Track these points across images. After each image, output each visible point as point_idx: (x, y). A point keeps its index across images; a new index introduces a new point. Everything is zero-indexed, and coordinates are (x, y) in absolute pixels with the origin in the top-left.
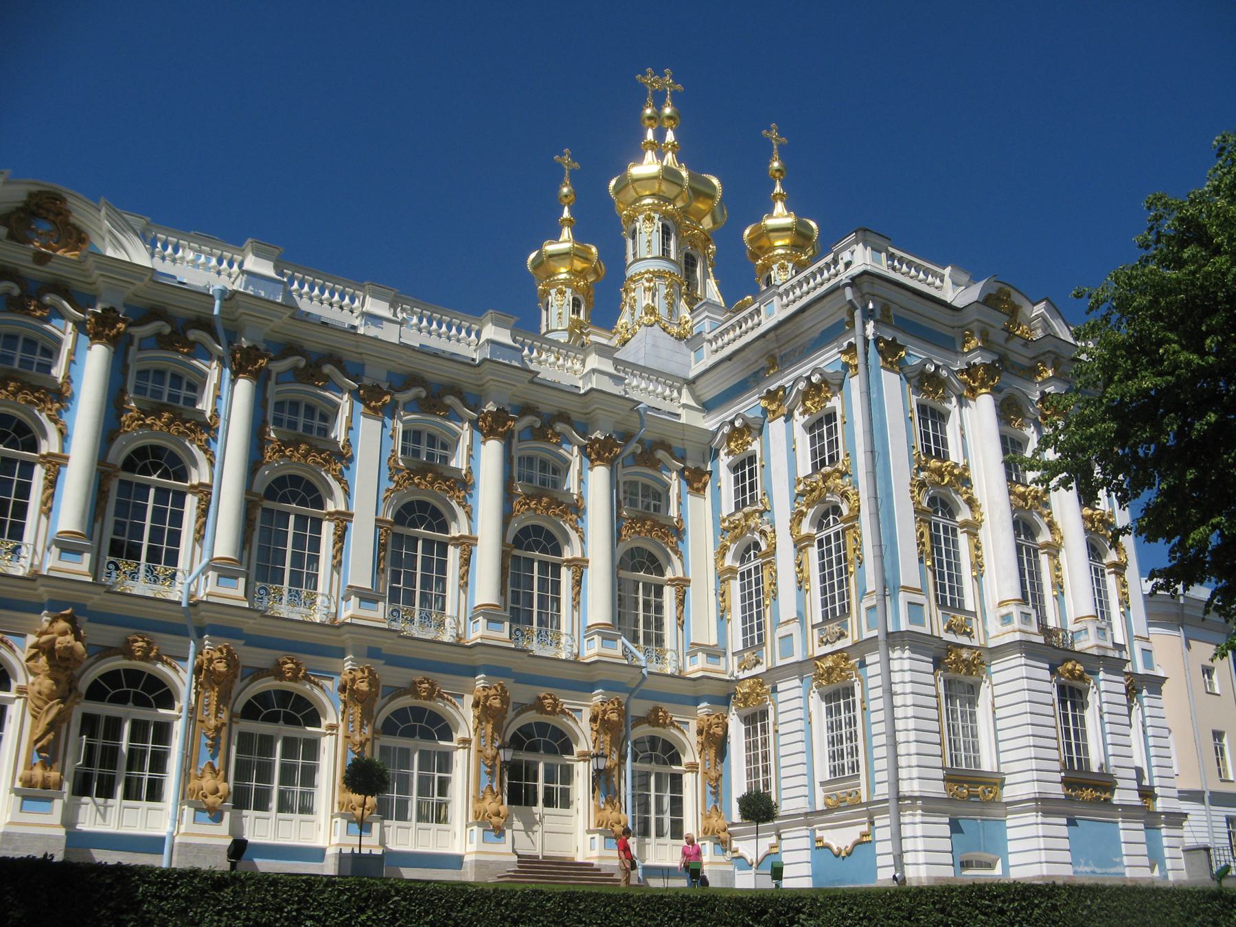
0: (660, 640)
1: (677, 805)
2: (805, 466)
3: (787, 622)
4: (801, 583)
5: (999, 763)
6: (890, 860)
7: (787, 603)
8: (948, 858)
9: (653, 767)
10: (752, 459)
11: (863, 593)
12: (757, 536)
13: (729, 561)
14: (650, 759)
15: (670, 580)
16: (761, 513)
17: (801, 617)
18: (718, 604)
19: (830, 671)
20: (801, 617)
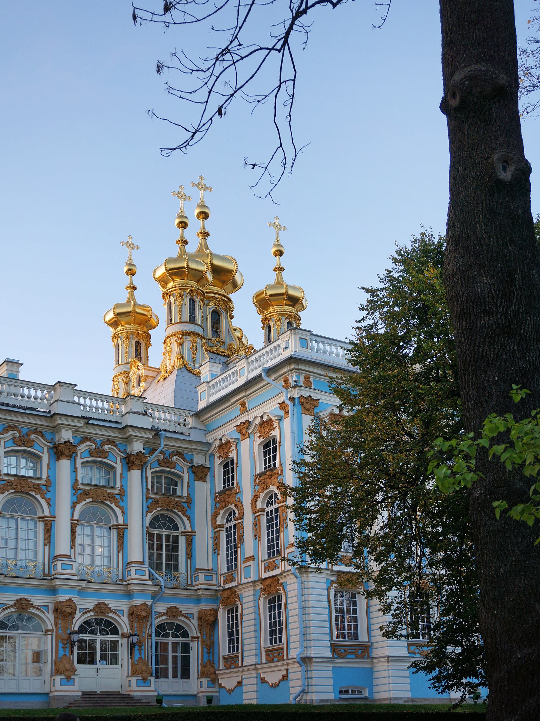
15: (182, 532)
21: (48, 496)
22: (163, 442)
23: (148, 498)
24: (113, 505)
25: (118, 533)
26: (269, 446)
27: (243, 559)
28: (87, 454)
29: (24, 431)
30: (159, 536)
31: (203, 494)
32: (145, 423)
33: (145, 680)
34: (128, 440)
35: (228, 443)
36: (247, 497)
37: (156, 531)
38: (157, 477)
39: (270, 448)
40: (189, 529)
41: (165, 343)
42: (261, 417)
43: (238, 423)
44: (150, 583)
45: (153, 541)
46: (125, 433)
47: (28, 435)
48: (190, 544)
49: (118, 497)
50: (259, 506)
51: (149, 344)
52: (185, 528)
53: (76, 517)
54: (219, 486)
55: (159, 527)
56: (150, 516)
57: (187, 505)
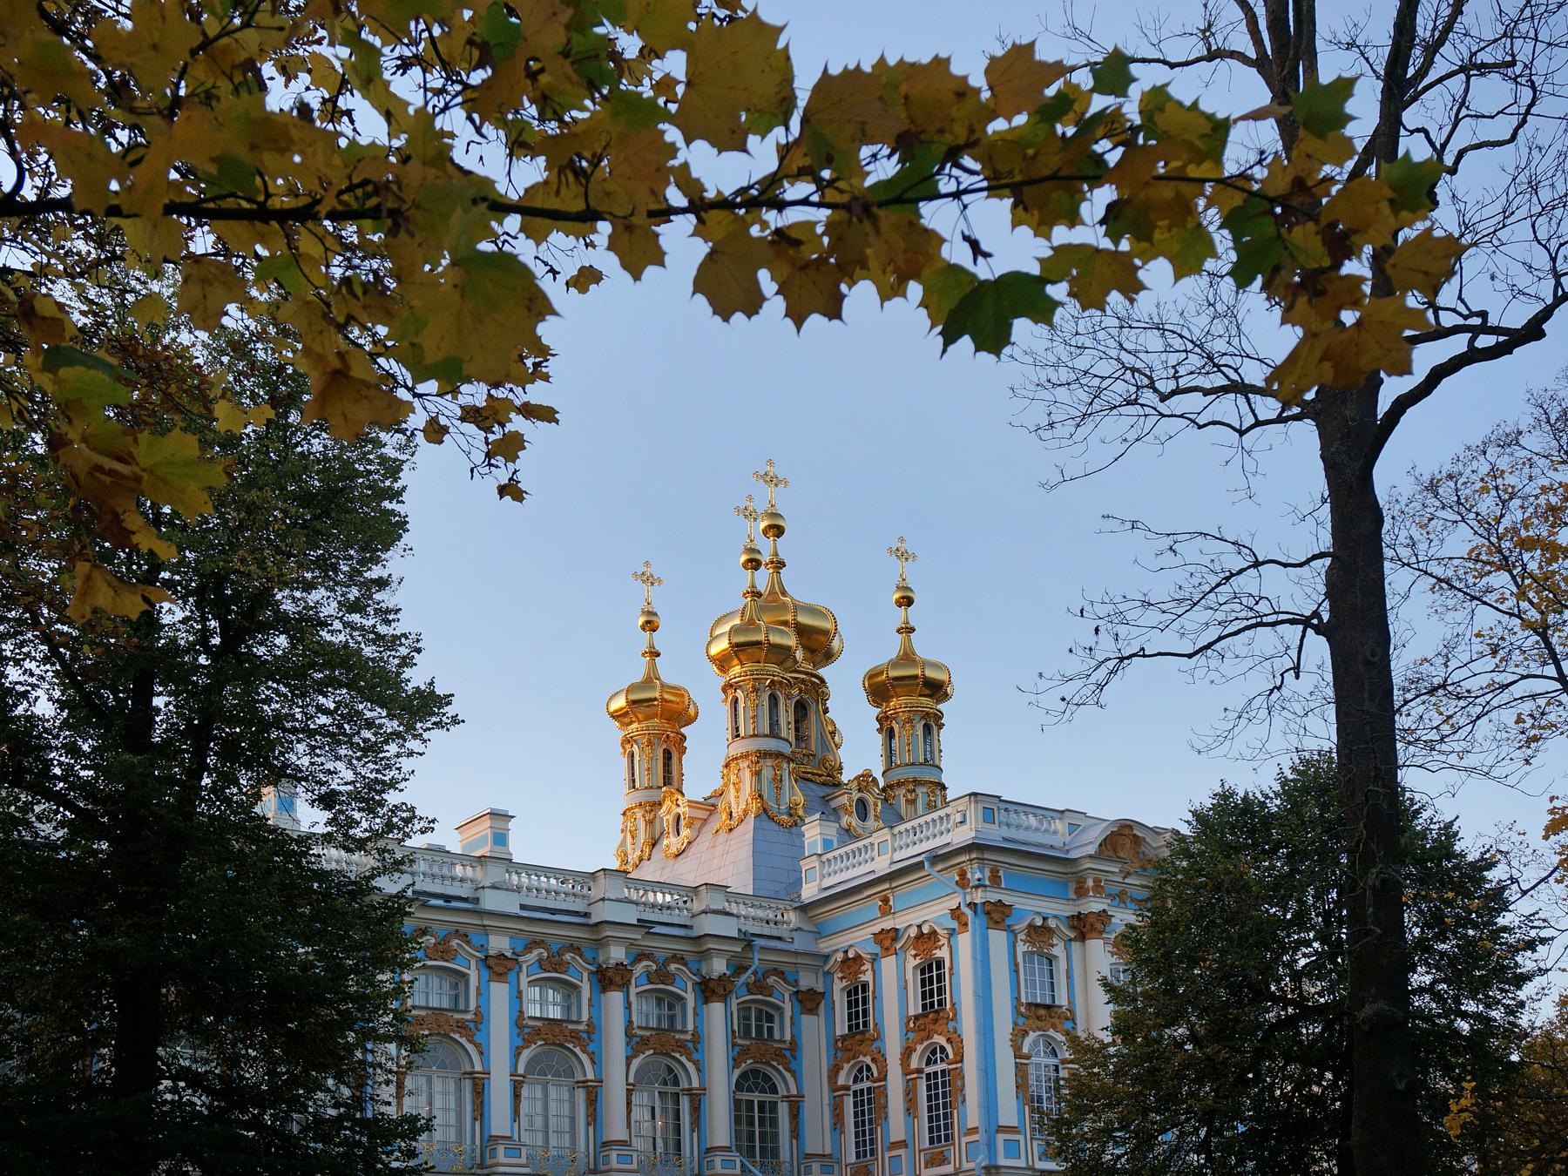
0: (775, 1153)
10: (865, 987)
12: (868, 1060)
13: (841, 1081)
21: (590, 1048)
22: (757, 956)
23: (734, 1045)
24: (683, 1059)
25: (691, 1101)
26: (931, 971)
27: (887, 1145)
29: (555, 948)
31: (815, 1037)
32: (728, 928)
34: (705, 955)
35: (858, 959)
36: (893, 1046)
37: (745, 1096)
38: (744, 1010)
39: (932, 976)
40: (794, 1091)
41: (727, 766)
42: (919, 927)
43: (877, 929)
45: (741, 1111)
46: (700, 945)
47: (560, 953)
48: (795, 1115)
49: (690, 1045)
50: (914, 1064)
51: (683, 751)
52: (788, 1090)
53: (631, 1080)
54: (842, 1028)
55: (750, 1090)
56: (737, 1072)
57: (790, 1054)
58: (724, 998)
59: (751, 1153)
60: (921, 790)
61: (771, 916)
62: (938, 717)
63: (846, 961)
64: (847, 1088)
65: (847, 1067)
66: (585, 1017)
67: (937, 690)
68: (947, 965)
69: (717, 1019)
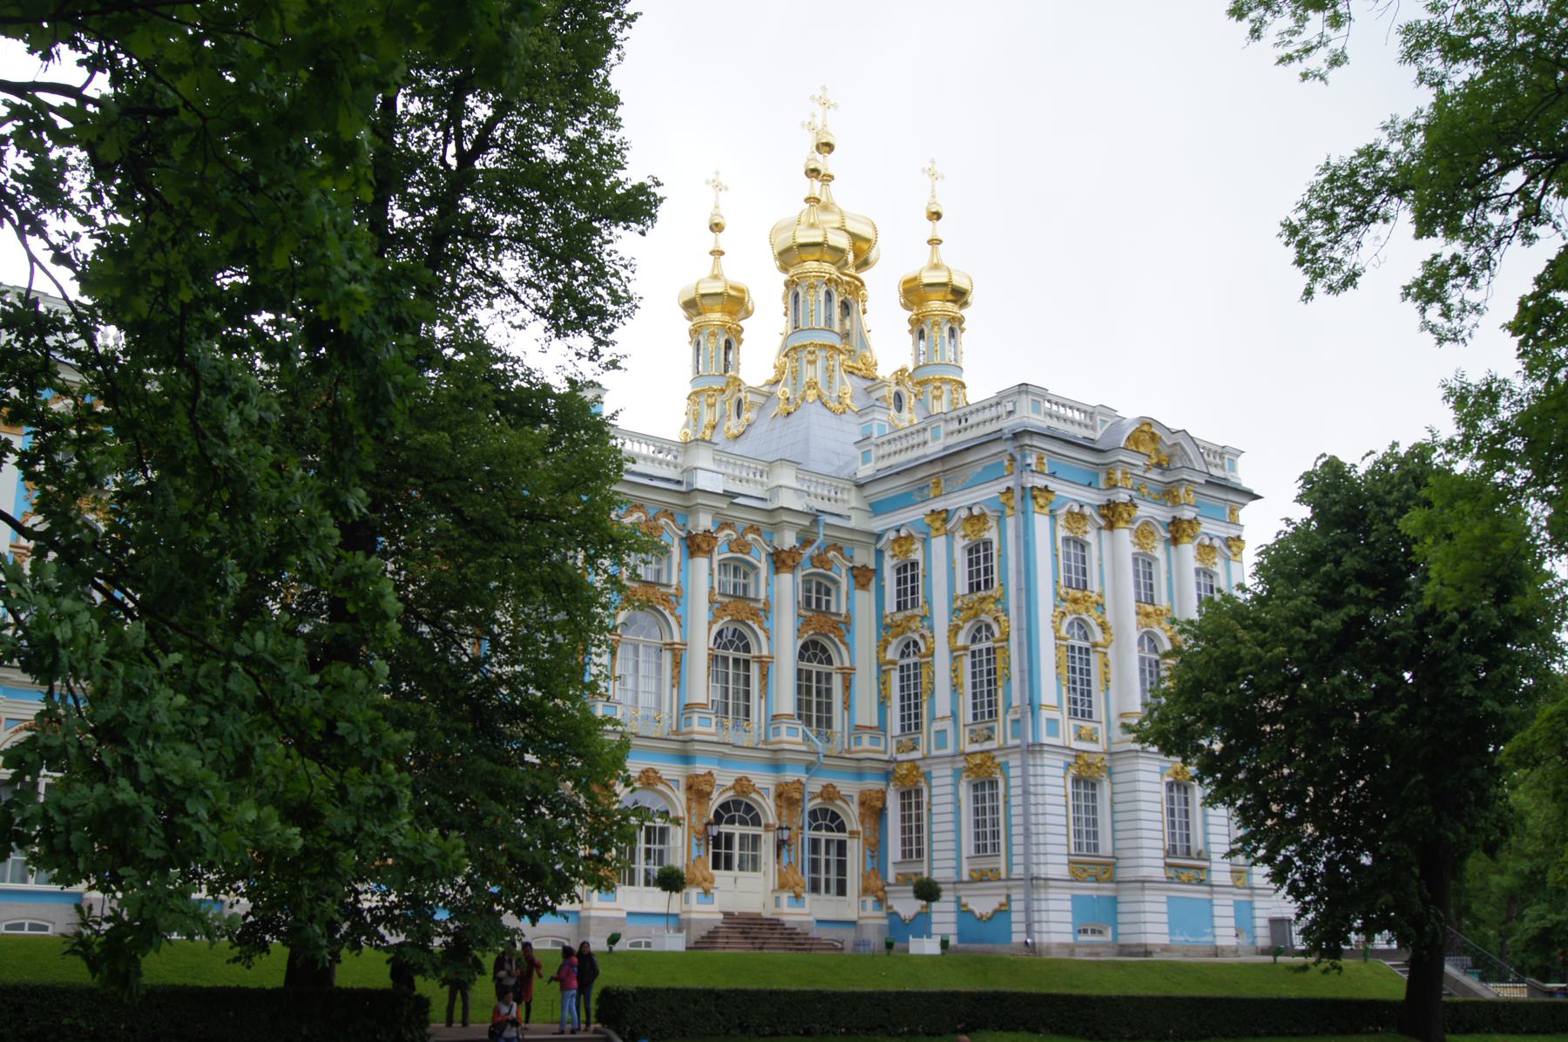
1: (842, 867)
2: (962, 587)
3: (943, 718)
4: (955, 687)
5: (1114, 849)
6: (1022, 927)
7: (943, 701)
8: (1069, 928)
9: (823, 835)
10: (914, 565)
11: (1008, 706)
14: (818, 828)
16: (923, 618)
17: (954, 715)
18: (879, 692)
19: (979, 766)
20: (954, 715)
22: (822, 531)
25: (761, 668)
28: (725, 548)
30: (809, 673)
31: (863, 610)
33: (797, 897)
34: (776, 527)
37: (805, 665)
38: (807, 580)
40: (847, 664)
44: (804, 748)
48: (847, 687)
51: (740, 342)
55: (809, 660)
56: (800, 642)
57: (842, 627)
58: (793, 569)
59: (808, 723)
60: (945, 388)
61: (826, 493)
62: (961, 321)
63: (898, 540)
64: (893, 663)
65: (895, 642)
66: (674, 581)
67: (959, 295)
68: (995, 545)
69: (787, 588)
